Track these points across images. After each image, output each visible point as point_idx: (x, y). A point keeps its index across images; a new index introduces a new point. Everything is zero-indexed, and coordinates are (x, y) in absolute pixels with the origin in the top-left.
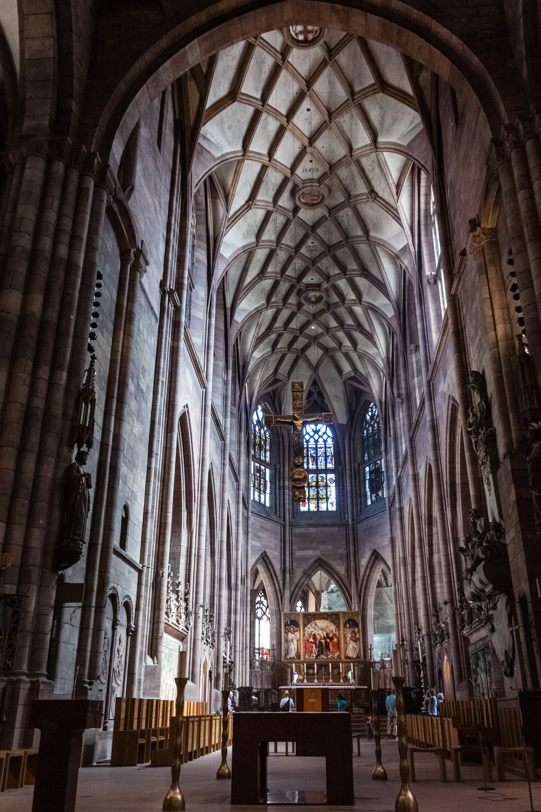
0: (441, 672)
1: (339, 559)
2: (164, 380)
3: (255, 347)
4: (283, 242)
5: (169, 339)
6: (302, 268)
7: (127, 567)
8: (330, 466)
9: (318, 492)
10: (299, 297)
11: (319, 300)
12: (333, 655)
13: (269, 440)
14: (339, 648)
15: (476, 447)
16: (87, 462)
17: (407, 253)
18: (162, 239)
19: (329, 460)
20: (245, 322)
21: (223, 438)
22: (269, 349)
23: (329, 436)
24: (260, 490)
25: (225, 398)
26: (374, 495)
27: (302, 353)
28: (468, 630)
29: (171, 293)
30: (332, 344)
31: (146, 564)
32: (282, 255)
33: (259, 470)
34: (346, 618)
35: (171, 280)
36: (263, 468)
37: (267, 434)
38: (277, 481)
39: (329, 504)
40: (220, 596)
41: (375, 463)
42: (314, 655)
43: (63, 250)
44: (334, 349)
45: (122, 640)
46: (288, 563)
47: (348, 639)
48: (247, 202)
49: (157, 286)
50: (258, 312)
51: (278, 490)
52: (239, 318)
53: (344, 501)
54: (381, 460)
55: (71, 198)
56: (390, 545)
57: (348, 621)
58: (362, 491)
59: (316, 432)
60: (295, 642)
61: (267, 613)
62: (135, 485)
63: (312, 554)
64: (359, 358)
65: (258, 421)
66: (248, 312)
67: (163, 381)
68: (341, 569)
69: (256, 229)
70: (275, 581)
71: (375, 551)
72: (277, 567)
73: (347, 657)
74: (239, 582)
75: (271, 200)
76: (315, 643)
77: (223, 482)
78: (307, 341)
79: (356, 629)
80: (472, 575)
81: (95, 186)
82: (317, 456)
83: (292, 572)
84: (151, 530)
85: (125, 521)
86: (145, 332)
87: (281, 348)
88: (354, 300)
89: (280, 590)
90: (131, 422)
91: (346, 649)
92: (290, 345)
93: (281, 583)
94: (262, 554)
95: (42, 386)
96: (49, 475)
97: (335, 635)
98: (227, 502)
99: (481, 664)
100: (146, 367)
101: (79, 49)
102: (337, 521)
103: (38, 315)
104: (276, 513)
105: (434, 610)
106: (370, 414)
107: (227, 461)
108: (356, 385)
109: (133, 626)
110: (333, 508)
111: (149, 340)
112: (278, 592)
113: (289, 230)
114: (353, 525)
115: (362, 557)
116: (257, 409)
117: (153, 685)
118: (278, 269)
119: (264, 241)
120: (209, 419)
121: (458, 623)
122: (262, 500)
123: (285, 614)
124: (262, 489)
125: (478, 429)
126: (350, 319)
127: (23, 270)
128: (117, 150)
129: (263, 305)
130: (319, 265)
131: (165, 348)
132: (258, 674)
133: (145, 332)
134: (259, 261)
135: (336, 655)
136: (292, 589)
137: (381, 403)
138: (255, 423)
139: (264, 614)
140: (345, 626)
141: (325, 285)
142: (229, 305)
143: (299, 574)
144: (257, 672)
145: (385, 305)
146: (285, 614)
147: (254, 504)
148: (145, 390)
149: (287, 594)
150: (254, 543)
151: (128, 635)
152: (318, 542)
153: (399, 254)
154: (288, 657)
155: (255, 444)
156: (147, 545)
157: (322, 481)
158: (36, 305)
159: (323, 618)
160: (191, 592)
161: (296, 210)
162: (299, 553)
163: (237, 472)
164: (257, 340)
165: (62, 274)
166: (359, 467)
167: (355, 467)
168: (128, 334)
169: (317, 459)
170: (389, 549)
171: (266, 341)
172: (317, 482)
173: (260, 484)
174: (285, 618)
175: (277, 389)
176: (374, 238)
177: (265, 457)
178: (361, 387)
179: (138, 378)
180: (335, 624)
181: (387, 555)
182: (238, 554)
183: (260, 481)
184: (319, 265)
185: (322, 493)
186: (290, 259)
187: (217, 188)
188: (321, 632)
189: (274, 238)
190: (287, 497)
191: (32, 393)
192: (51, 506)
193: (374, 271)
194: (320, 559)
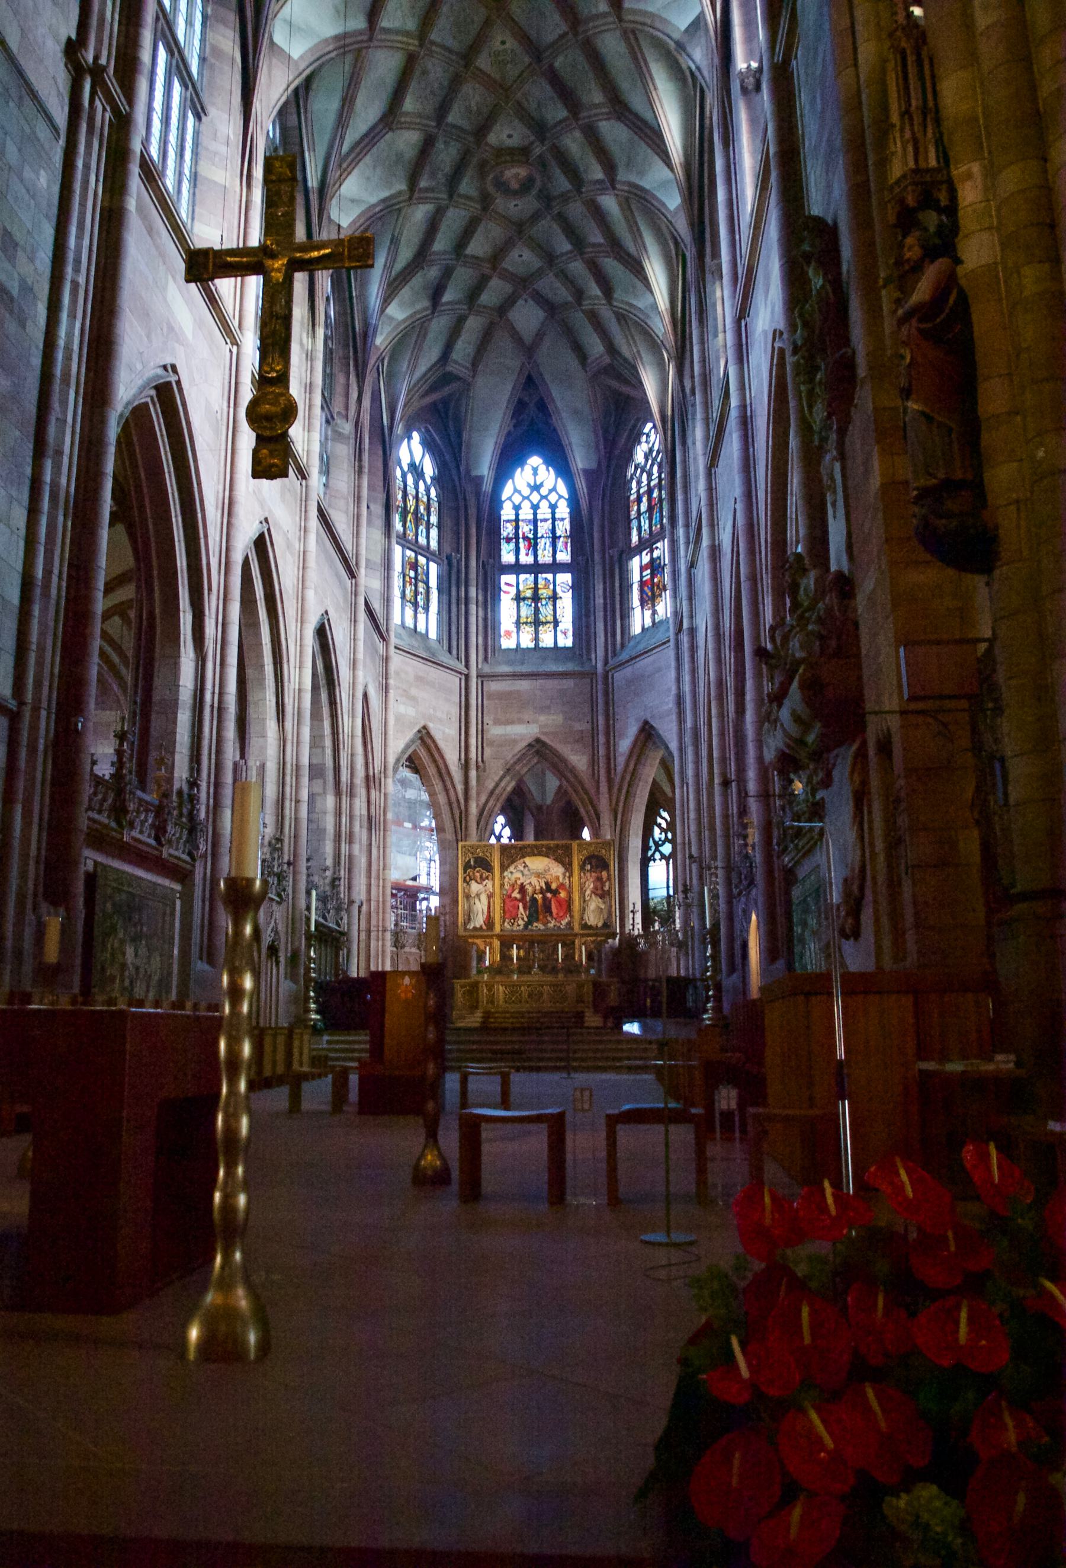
5: (95, 184)
8: (564, 557)
9: (537, 611)
11: (526, 186)
12: (556, 923)
13: (436, 505)
14: (569, 909)
17: (701, 33)
19: (560, 545)
23: (561, 497)
24: (416, 605)
28: (793, 854)
30: (562, 294)
32: (436, 71)
33: (414, 566)
36: (422, 560)
37: (433, 493)
39: (559, 633)
40: (297, 801)
42: (521, 922)
47: (588, 892)
49: (53, 51)
53: (588, 627)
56: (675, 710)
57: (589, 859)
59: (536, 488)
64: (618, 320)
65: (413, 466)
66: (363, 207)
67: (75, 285)
68: (579, 761)
70: (448, 783)
71: (646, 723)
73: (585, 926)
76: (522, 900)
78: (508, 288)
79: (604, 874)
82: (536, 538)
88: (598, 182)
91: (583, 910)
93: (460, 787)
94: (419, 731)
97: (562, 886)
100: (18, 236)
102: (570, 667)
104: (450, 652)
108: (615, 384)
110: (566, 641)
111: (28, 173)
112: (455, 805)
115: (622, 736)
116: (410, 438)
118: (430, 108)
119: (387, 31)
122: (421, 628)
124: (421, 603)
126: (597, 232)
129: (400, 193)
135: (564, 922)
136: (483, 799)
138: (406, 469)
140: (582, 868)
144: (410, 953)
147: (401, 631)
152: (535, 708)
153: (685, 40)
154: (471, 926)
157: (546, 587)
159: (540, 854)
160: (204, 785)
167: (611, 557)
169: (536, 544)
171: (417, 281)
172: (536, 589)
173: (416, 593)
174: (465, 854)
175: (450, 395)
176: (635, 12)
177: (428, 537)
178: (625, 389)
181: (668, 730)
183: (416, 586)
185: (546, 612)
186: (455, 84)
188: (534, 881)
189: (411, 25)
190: (473, 620)
193: (637, 103)
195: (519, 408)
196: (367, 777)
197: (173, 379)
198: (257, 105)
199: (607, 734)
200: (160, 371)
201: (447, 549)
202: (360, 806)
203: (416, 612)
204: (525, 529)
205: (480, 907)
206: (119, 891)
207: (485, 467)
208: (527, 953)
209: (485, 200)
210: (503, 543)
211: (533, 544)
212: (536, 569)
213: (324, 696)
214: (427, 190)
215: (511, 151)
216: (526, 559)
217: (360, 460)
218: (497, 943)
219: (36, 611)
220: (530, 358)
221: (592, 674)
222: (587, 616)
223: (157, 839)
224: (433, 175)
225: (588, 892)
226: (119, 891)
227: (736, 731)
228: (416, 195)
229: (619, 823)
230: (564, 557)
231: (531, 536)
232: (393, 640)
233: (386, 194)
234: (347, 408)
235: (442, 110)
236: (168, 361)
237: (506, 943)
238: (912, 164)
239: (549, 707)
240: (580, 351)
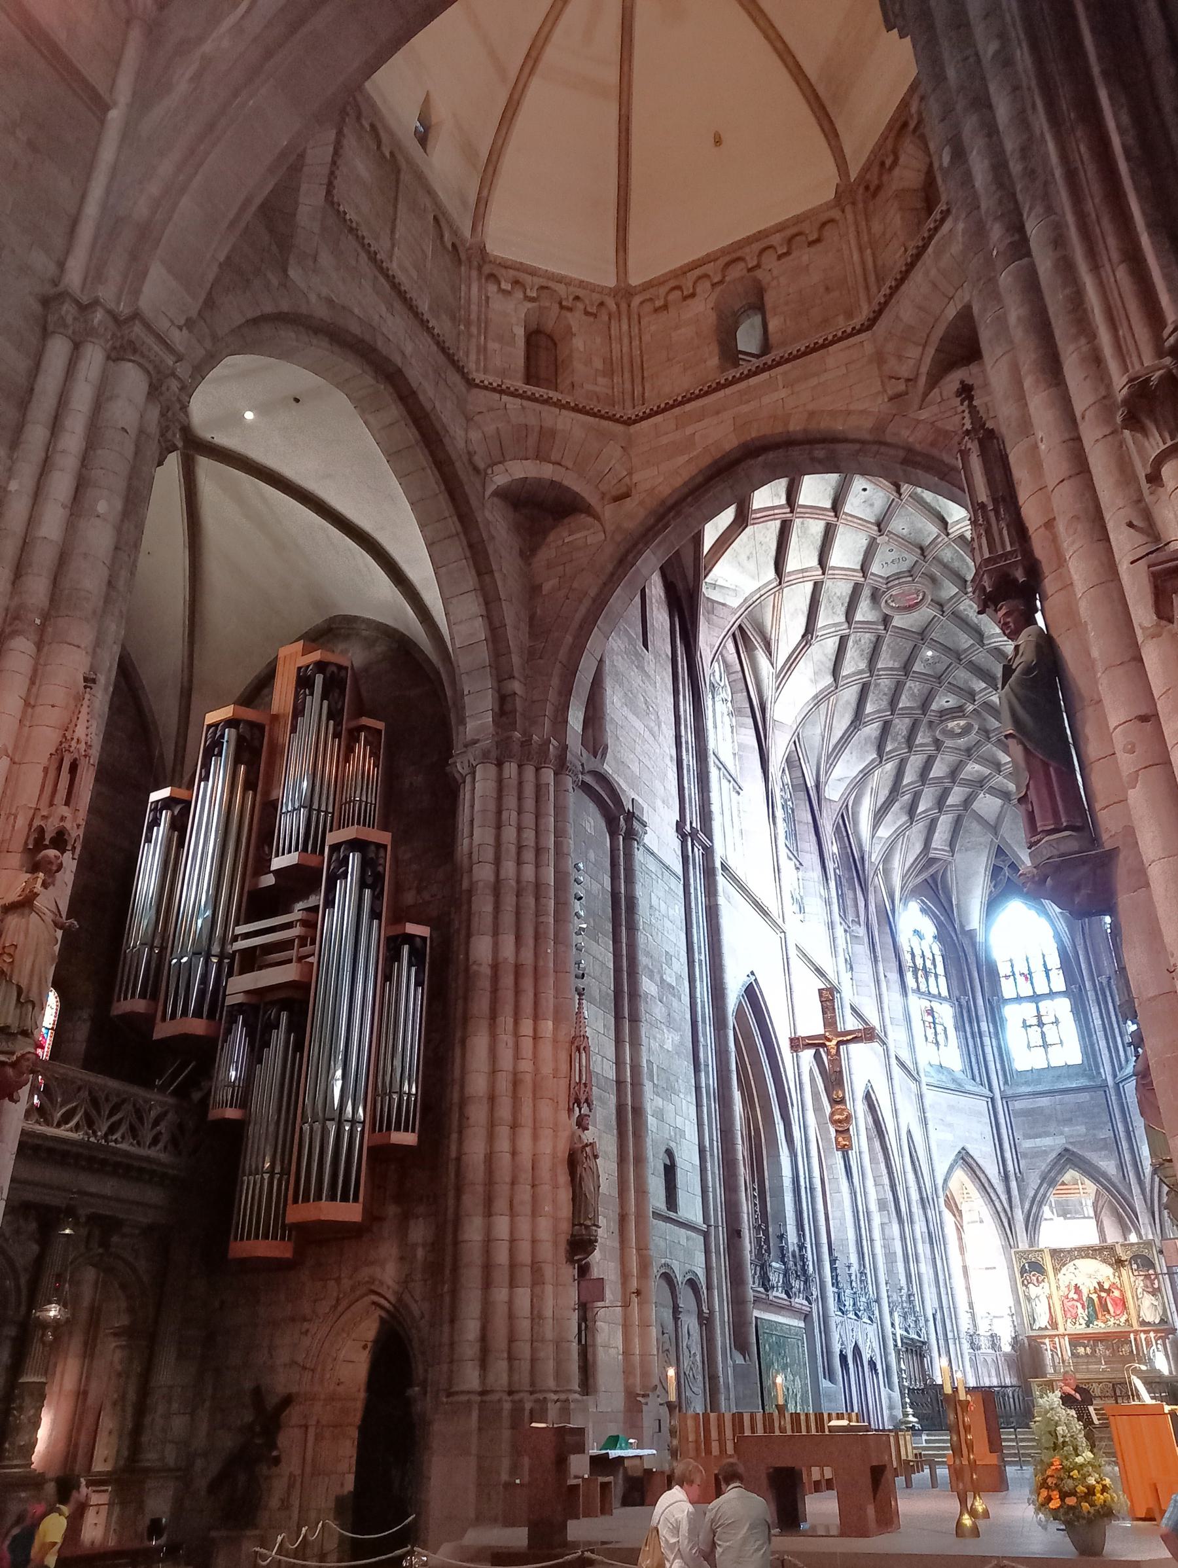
1: (1101, 1149)
3: (876, 825)
4: (879, 666)
5: (701, 898)
7: (683, 1232)
9: (1043, 1034)
10: (934, 731)
11: (966, 730)
18: (669, 763)
22: (905, 818)
27: (966, 809)
29: (693, 834)
33: (931, 1012)
35: (691, 814)
37: (936, 948)
38: (967, 1025)
42: (1083, 1322)
43: (529, 872)
47: (1140, 1290)
48: (803, 636)
50: (866, 773)
52: (834, 791)
53: (1092, 1045)
55: (529, 804)
63: (1052, 1143)
66: (848, 781)
68: (1109, 1166)
69: (831, 665)
72: (992, 1171)
73: (1143, 1323)
75: (843, 619)
76: (1080, 1299)
79: (1151, 1272)
81: (556, 774)
82: (1030, 973)
84: (713, 1173)
85: (670, 1171)
87: (923, 812)
92: (940, 802)
93: (1004, 1197)
95: (527, 1044)
96: (548, 1151)
101: (510, 613)
102: (1083, 1082)
103: (512, 960)
104: (974, 1079)
111: (671, 912)
112: (1002, 1215)
113: (884, 648)
118: (884, 704)
127: (489, 908)
128: (576, 719)
129: (873, 761)
131: (697, 913)
132: (989, 1360)
134: (848, 702)
135: (1123, 1319)
136: (1027, 1206)
141: (970, 708)
142: (811, 783)
143: (1033, 1181)
147: (928, 1069)
149: (1019, 1216)
151: (701, 1324)
154: (1036, 1327)
158: (508, 949)
159: (1087, 1256)
161: (886, 620)
162: (1026, 1144)
165: (531, 901)
167: (1101, 983)
168: (632, 928)
172: (1039, 1016)
187: (749, 636)
189: (863, 665)
190: (988, 1050)
191: (517, 1057)
192: (556, 1187)
194: (1066, 1150)
195: (996, 872)
196: (922, 1199)
198: (771, 769)
201: (957, 993)
202: (920, 1227)
207: (974, 920)
209: (938, 744)
211: (1029, 977)
212: (1036, 998)
213: (877, 1144)
215: (951, 710)
216: (1025, 990)
217: (874, 952)
219: (709, 1165)
220: (996, 834)
221: (1104, 1086)
222: (1090, 1036)
223: (787, 1293)
225: (1140, 1290)
229: (1157, 1221)
230: (1059, 983)
231: (1026, 972)
232: (924, 1080)
234: (858, 916)
239: (1071, 1120)
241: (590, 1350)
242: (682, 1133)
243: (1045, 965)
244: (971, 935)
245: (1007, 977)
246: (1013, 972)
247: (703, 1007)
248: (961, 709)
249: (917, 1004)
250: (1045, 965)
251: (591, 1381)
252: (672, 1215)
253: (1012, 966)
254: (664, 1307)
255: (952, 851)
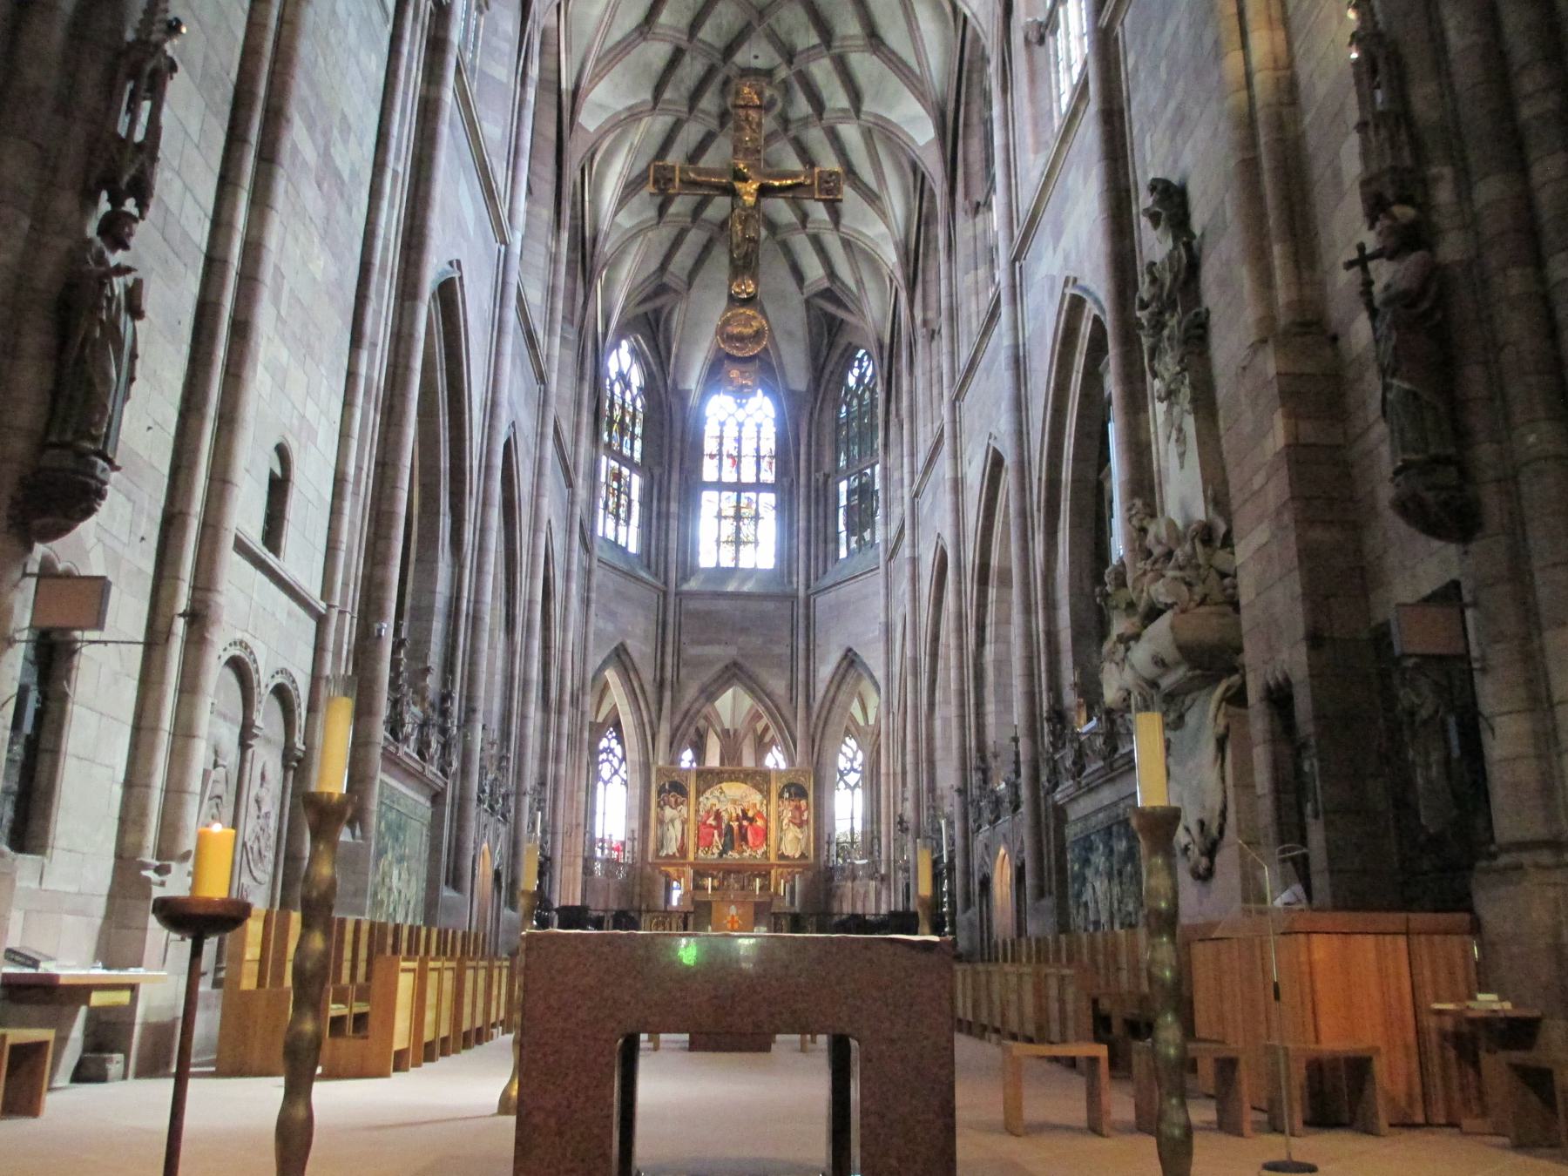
0: (986, 883)
2: (400, 169)
3: (622, 202)
5: (417, 75)
6: (737, 27)
9: (738, 529)
13: (640, 416)
15: (1151, 359)
16: (133, 242)
19: (764, 464)
20: (602, 133)
21: (541, 378)
22: (652, 213)
24: (617, 517)
25: (551, 291)
26: (854, 539)
31: (337, 602)
33: (618, 477)
34: (785, 781)
36: (625, 471)
37: (639, 404)
41: (861, 474)
42: (716, 851)
44: (790, 227)
45: (269, 775)
46: (669, 669)
50: (633, 115)
51: (654, 521)
52: (590, 120)
54: (872, 467)
56: (883, 638)
57: (788, 786)
58: (830, 530)
60: (677, 826)
61: (622, 772)
62: (310, 404)
63: (720, 653)
67: (395, 172)
68: (778, 686)
71: (850, 650)
73: (782, 856)
74: (567, 698)
76: (718, 827)
77: (539, 474)
79: (803, 803)
80: (1127, 649)
82: (739, 456)
83: (677, 686)
84: (352, 523)
85: (278, 488)
86: (352, 30)
87: (678, 215)
88: (843, 110)
89: (651, 723)
90: (302, 238)
93: (653, 708)
97: (759, 814)
98: (545, 527)
99: (1099, 859)
100: (352, 119)
104: (649, 567)
105: (978, 761)
106: (856, 372)
107: (550, 431)
108: (831, 308)
109: (300, 745)
111: (363, 56)
114: (808, 597)
117: (351, 888)
120: (511, 316)
121: (1044, 778)
123: (659, 770)
124: (623, 515)
125: (1161, 313)
129: (644, 102)
130: (772, 21)
131: (406, 93)
133: (352, 30)
135: (760, 852)
137: (881, 346)
138: (613, 376)
139: (616, 772)
140: (781, 796)
145: (913, 120)
146: (659, 770)
148: (346, 176)
150: (601, 624)
151: (286, 767)
154: (663, 853)
155: (611, 422)
156: (342, 556)
157: (748, 506)
159: (737, 780)
160: (456, 696)
163: (570, 463)
164: (626, 187)
166: (826, 482)
170: (881, 646)
173: (618, 505)
175: (662, 307)
177: (632, 449)
178: (841, 314)
179: (326, 133)
180: (761, 791)
181: (874, 659)
182: (567, 638)
184: (772, 21)
188: (731, 808)
194: (735, 664)
197: (457, 276)
199: (807, 659)
200: (448, 267)
203: (617, 524)
204: (730, 446)
205: (674, 833)
206: (391, 808)
207: (693, 381)
208: (721, 883)
210: (706, 460)
211: (737, 461)
212: (739, 487)
214: (670, 102)
215: (757, 72)
216: (729, 476)
218: (690, 872)
223: (420, 753)
224: (677, 89)
226: (391, 808)
227: (975, 665)
228: (660, 106)
230: (768, 476)
231: (735, 453)
232: (597, 552)
233: (631, 102)
235: (695, 26)
236: (455, 256)
237: (700, 872)
238: (1389, 162)
240: (798, 274)
241: (45, 759)
242: (312, 434)
243: (758, 450)
244: (683, 396)
245: (712, 456)
246: (720, 451)
247: (386, 248)
248: (769, 73)
249: (606, 464)
250: (758, 450)
251: (34, 826)
252: (270, 558)
253: (721, 444)
254: (224, 717)
255: (690, 285)
